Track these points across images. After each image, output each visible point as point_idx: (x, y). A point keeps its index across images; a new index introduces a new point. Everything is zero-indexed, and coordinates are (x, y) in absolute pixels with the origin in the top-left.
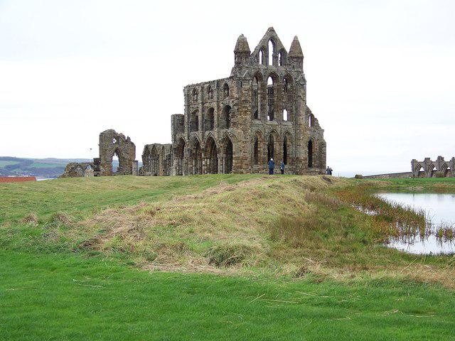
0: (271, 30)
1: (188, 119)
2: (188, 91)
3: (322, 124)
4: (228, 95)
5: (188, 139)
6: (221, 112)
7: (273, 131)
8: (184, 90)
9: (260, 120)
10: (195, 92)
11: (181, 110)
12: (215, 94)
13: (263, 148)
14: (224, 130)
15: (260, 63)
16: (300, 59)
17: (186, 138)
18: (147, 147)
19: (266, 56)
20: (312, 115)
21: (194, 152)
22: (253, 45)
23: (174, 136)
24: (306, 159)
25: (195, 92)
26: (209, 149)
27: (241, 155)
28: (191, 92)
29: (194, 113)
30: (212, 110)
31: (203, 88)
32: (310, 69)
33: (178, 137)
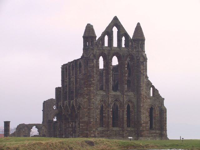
0: (116, 19)
3: (162, 94)
5: (63, 107)
7: (116, 100)
9: (104, 91)
11: (60, 86)
15: (106, 44)
17: (62, 106)
20: (153, 87)
24: (147, 123)
27: (86, 119)
30: (73, 84)
31: (69, 66)
32: (149, 49)
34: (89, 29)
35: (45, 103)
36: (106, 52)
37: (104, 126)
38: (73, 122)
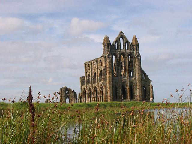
0: (122, 32)
1: (86, 78)
2: (86, 65)
3: (150, 77)
5: (87, 88)
6: (99, 74)
11: (84, 75)
13: (120, 90)
15: (117, 48)
16: (137, 46)
18: (79, 94)
19: (119, 46)
20: (145, 74)
21: (90, 94)
22: (112, 40)
23: (81, 87)
25: (88, 65)
26: (95, 92)
28: (87, 65)
29: (89, 75)
31: (91, 63)
33: (83, 87)
34: (107, 39)
37: (118, 98)
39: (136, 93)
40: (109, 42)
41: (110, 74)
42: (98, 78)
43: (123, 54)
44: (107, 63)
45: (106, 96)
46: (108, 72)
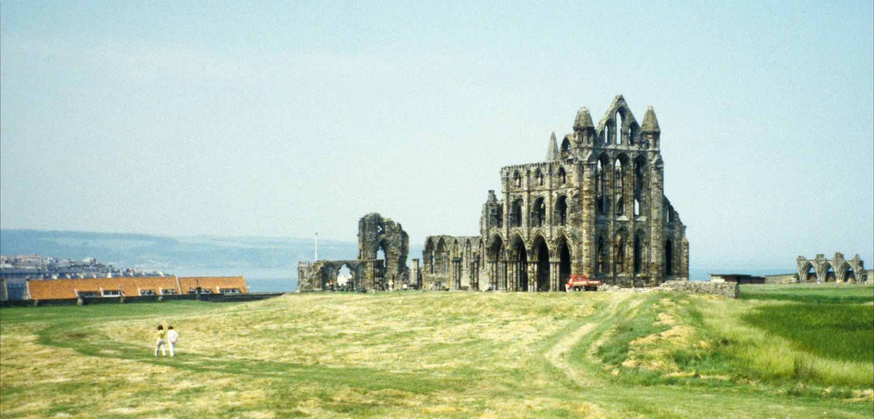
0: (621, 99)
2: (508, 174)
4: (564, 182)
6: (554, 205)
8: (501, 172)
10: (517, 176)
12: (547, 180)
14: (560, 227)
16: (656, 135)
17: (505, 235)
18: (430, 241)
19: (612, 133)
20: (671, 208)
22: (598, 121)
28: (512, 175)
30: (540, 200)
31: (529, 172)
32: (668, 147)
33: (493, 232)
35: (363, 221)
36: (610, 154)
38: (534, 263)
39: (649, 256)
40: (590, 125)
41: (590, 209)
42: (551, 215)
43: (623, 157)
44: (586, 179)
45: (579, 265)
46: (585, 202)
